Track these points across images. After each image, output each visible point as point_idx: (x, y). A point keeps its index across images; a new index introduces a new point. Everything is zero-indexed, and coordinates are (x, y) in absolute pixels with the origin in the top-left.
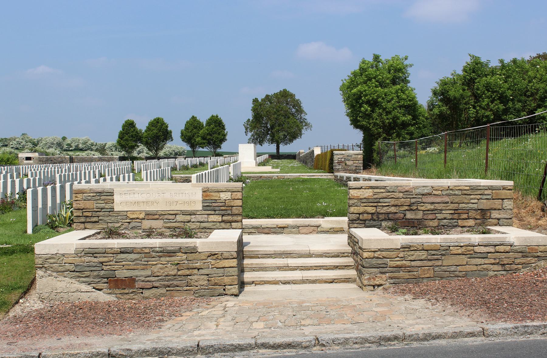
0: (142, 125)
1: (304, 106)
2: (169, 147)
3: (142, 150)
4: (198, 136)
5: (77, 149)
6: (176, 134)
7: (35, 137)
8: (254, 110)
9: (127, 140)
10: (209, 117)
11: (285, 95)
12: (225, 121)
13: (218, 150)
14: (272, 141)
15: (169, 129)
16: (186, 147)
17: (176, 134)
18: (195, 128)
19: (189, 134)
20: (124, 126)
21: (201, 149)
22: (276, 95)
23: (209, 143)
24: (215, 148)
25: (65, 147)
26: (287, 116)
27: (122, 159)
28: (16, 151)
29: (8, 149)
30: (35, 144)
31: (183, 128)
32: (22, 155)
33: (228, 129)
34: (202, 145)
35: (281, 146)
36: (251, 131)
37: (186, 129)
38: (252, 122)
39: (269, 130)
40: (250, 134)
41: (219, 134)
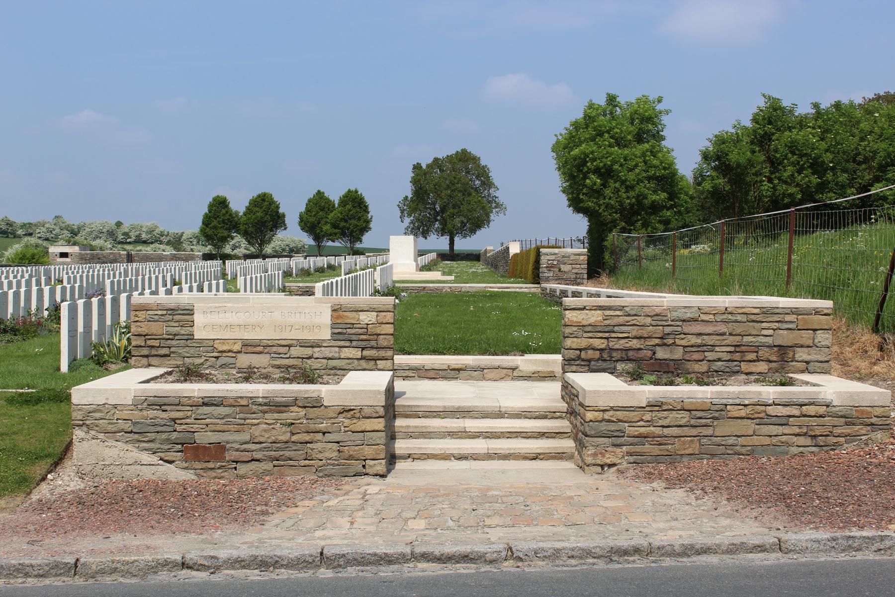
0: (239, 205)
1: (495, 176)
3: (239, 243)
4: (326, 223)
5: (139, 241)
6: (292, 219)
7: (74, 221)
8: (415, 181)
9: (215, 228)
10: (343, 192)
11: (464, 158)
12: (368, 200)
13: (358, 245)
14: (443, 232)
15: (281, 211)
16: (307, 240)
17: (292, 219)
19: (312, 219)
20: (211, 206)
21: (330, 243)
23: (343, 234)
25: (120, 237)
26: (466, 191)
27: (207, 257)
28: (45, 243)
29: (33, 240)
30: (74, 233)
31: (303, 209)
32: (54, 250)
33: (373, 211)
34: (332, 237)
35: (457, 239)
36: (409, 215)
37: (308, 210)
38: (412, 200)
40: (407, 220)
41: (359, 219)
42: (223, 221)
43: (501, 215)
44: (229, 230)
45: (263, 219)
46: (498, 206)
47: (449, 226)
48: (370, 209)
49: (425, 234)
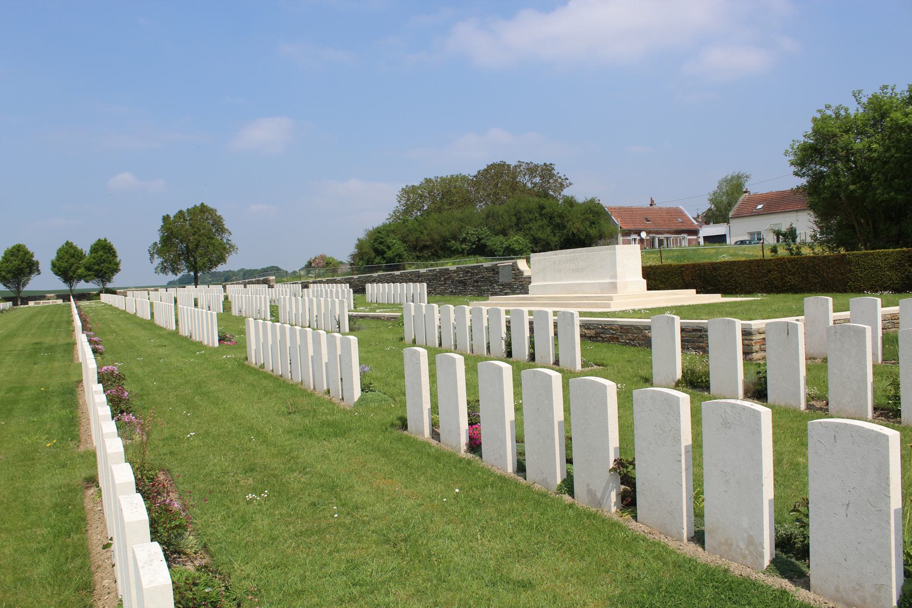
2: (34, 284)
11: (203, 209)
12: (116, 247)
16: (59, 285)
31: (54, 256)
33: (120, 256)
37: (59, 258)
41: (110, 263)
48: (118, 253)
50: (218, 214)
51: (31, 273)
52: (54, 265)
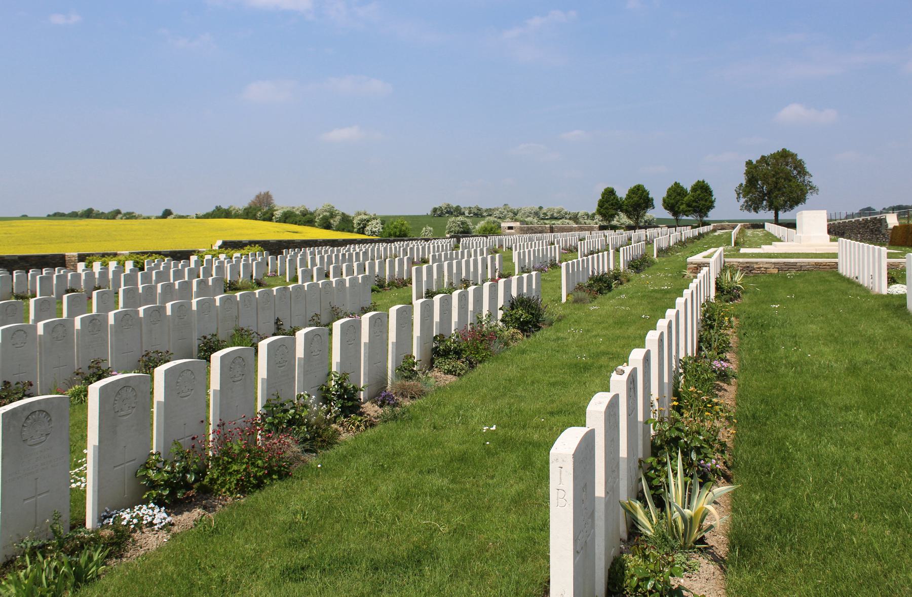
0: (622, 193)
1: (808, 167)
2: (650, 214)
3: (623, 218)
4: (682, 204)
6: (658, 202)
7: (515, 207)
8: (748, 173)
9: (606, 208)
10: (694, 182)
11: (784, 155)
12: (712, 187)
13: (705, 219)
15: (650, 196)
16: (668, 215)
17: (658, 202)
18: (679, 194)
19: (672, 201)
20: (604, 194)
21: (685, 217)
22: (773, 156)
23: (695, 211)
24: (701, 217)
25: (542, 216)
26: (788, 178)
27: (602, 228)
28: (499, 220)
29: (492, 219)
30: (515, 214)
31: (665, 195)
32: (504, 225)
33: (716, 195)
34: (686, 213)
35: (780, 213)
36: (744, 197)
37: (669, 195)
38: (746, 186)
39: (766, 195)
40: (742, 200)
41: (706, 200)
42: (612, 204)
43: (815, 195)
44: (616, 210)
45: (639, 201)
46: (812, 188)
47: (775, 203)
48: (713, 193)
49: (756, 210)
50: (799, 158)
51: (647, 207)
52: (664, 201)
